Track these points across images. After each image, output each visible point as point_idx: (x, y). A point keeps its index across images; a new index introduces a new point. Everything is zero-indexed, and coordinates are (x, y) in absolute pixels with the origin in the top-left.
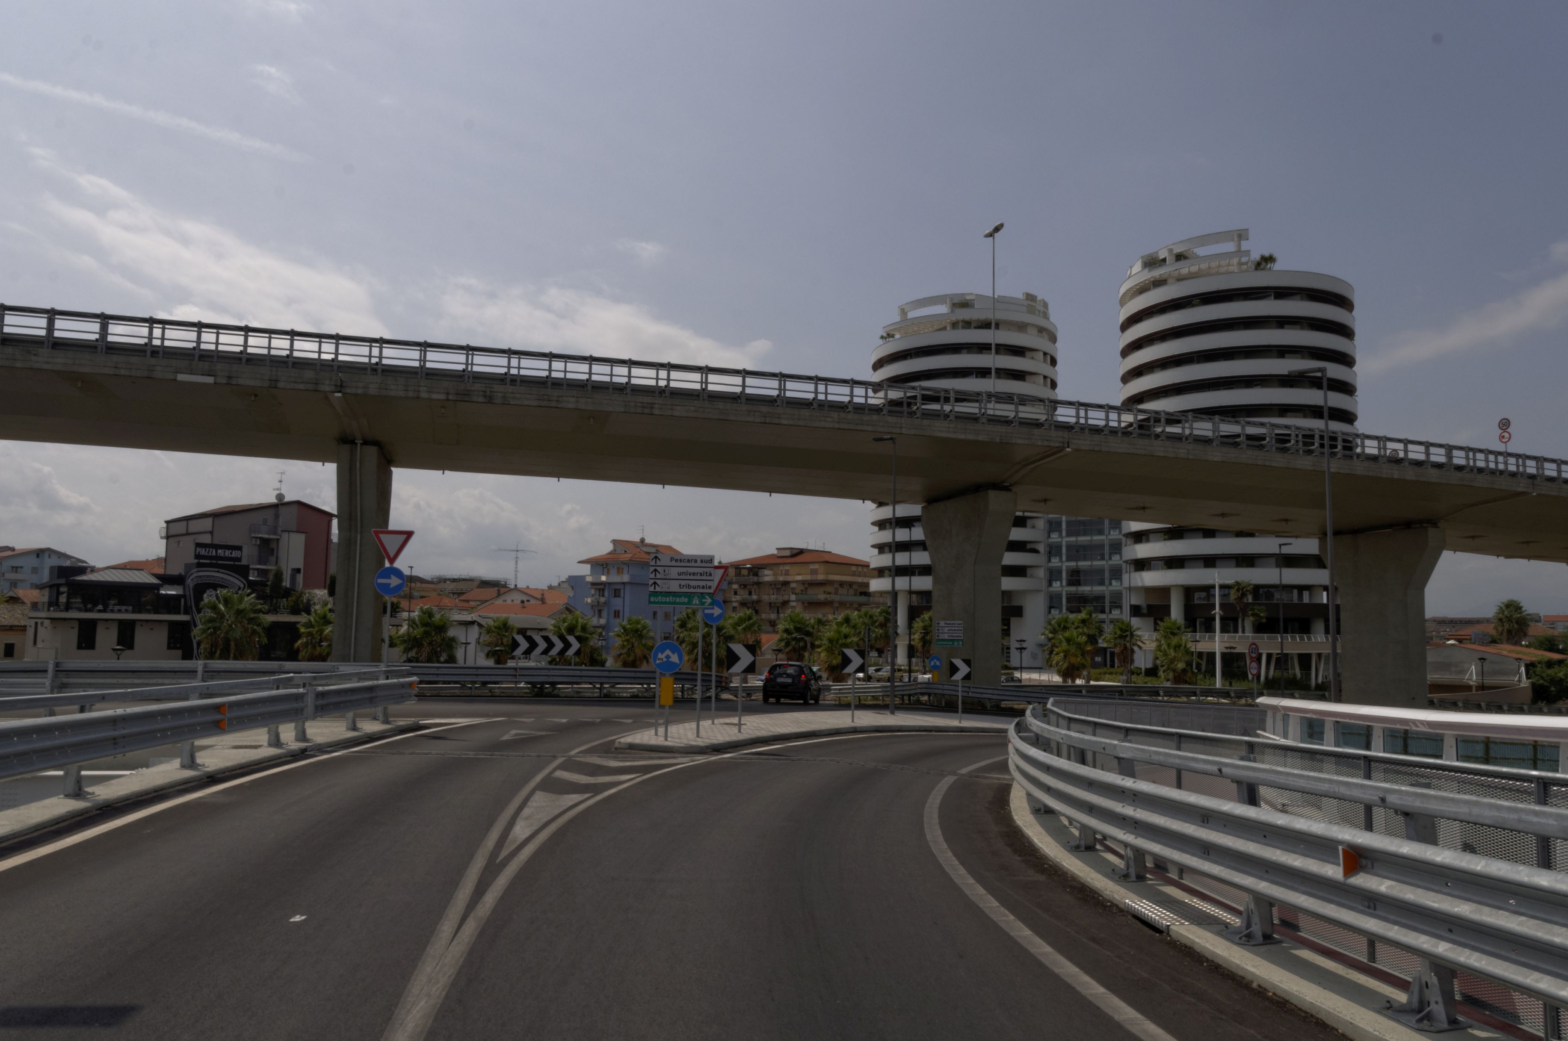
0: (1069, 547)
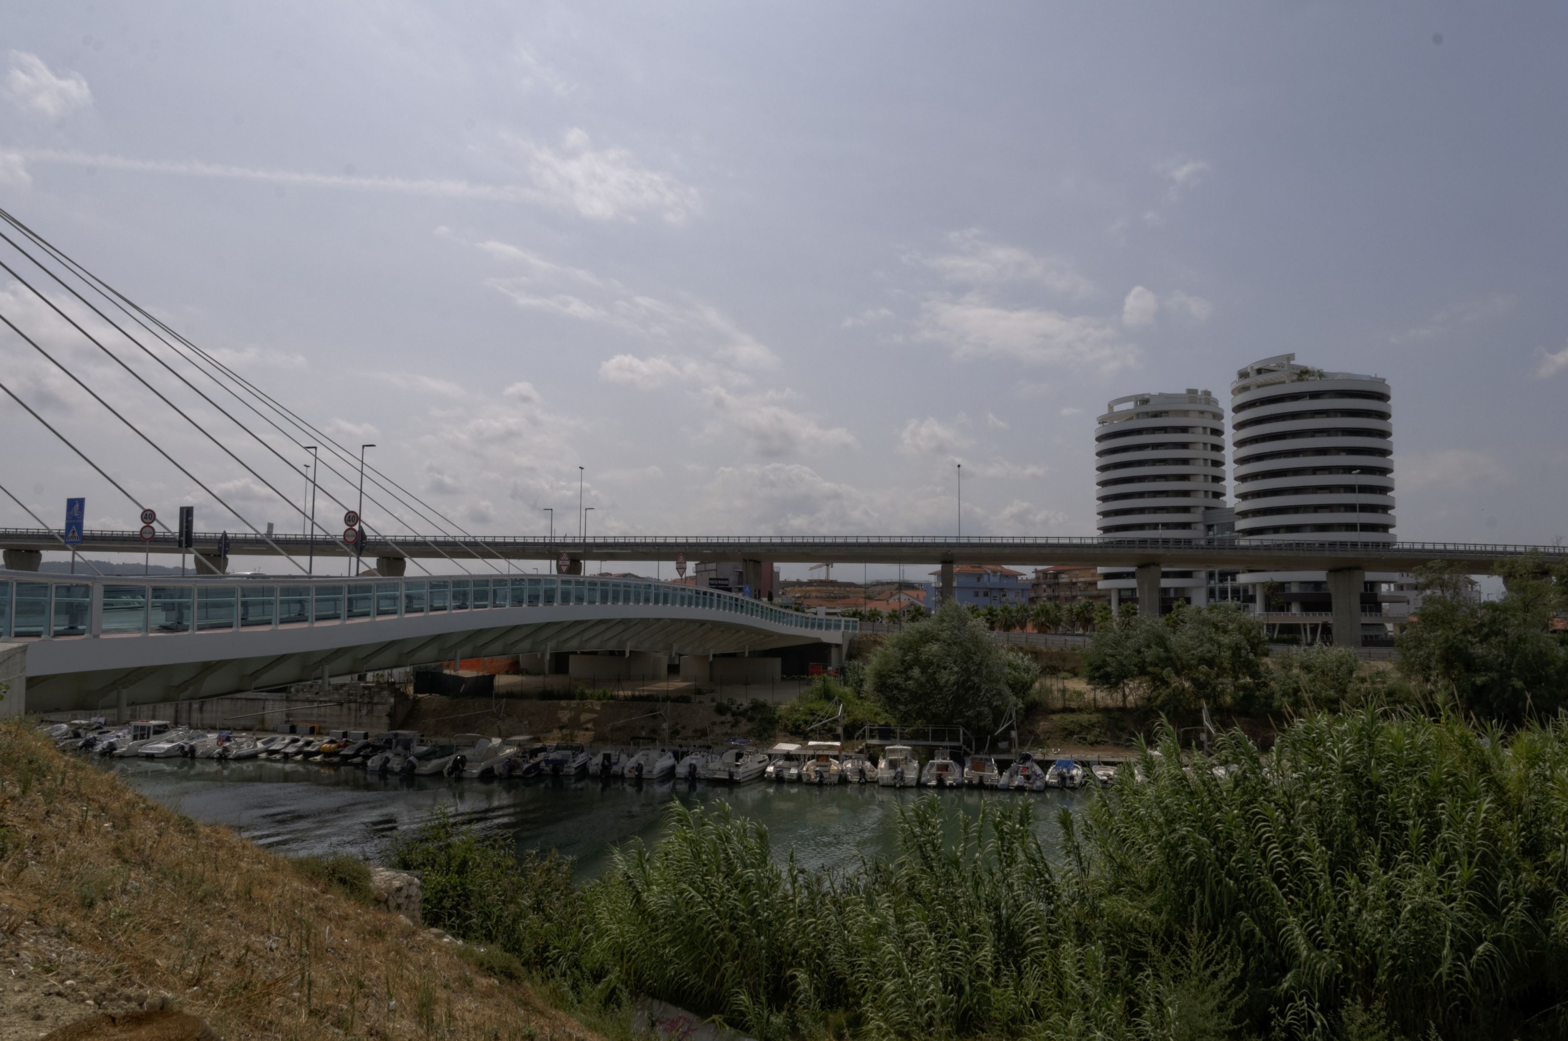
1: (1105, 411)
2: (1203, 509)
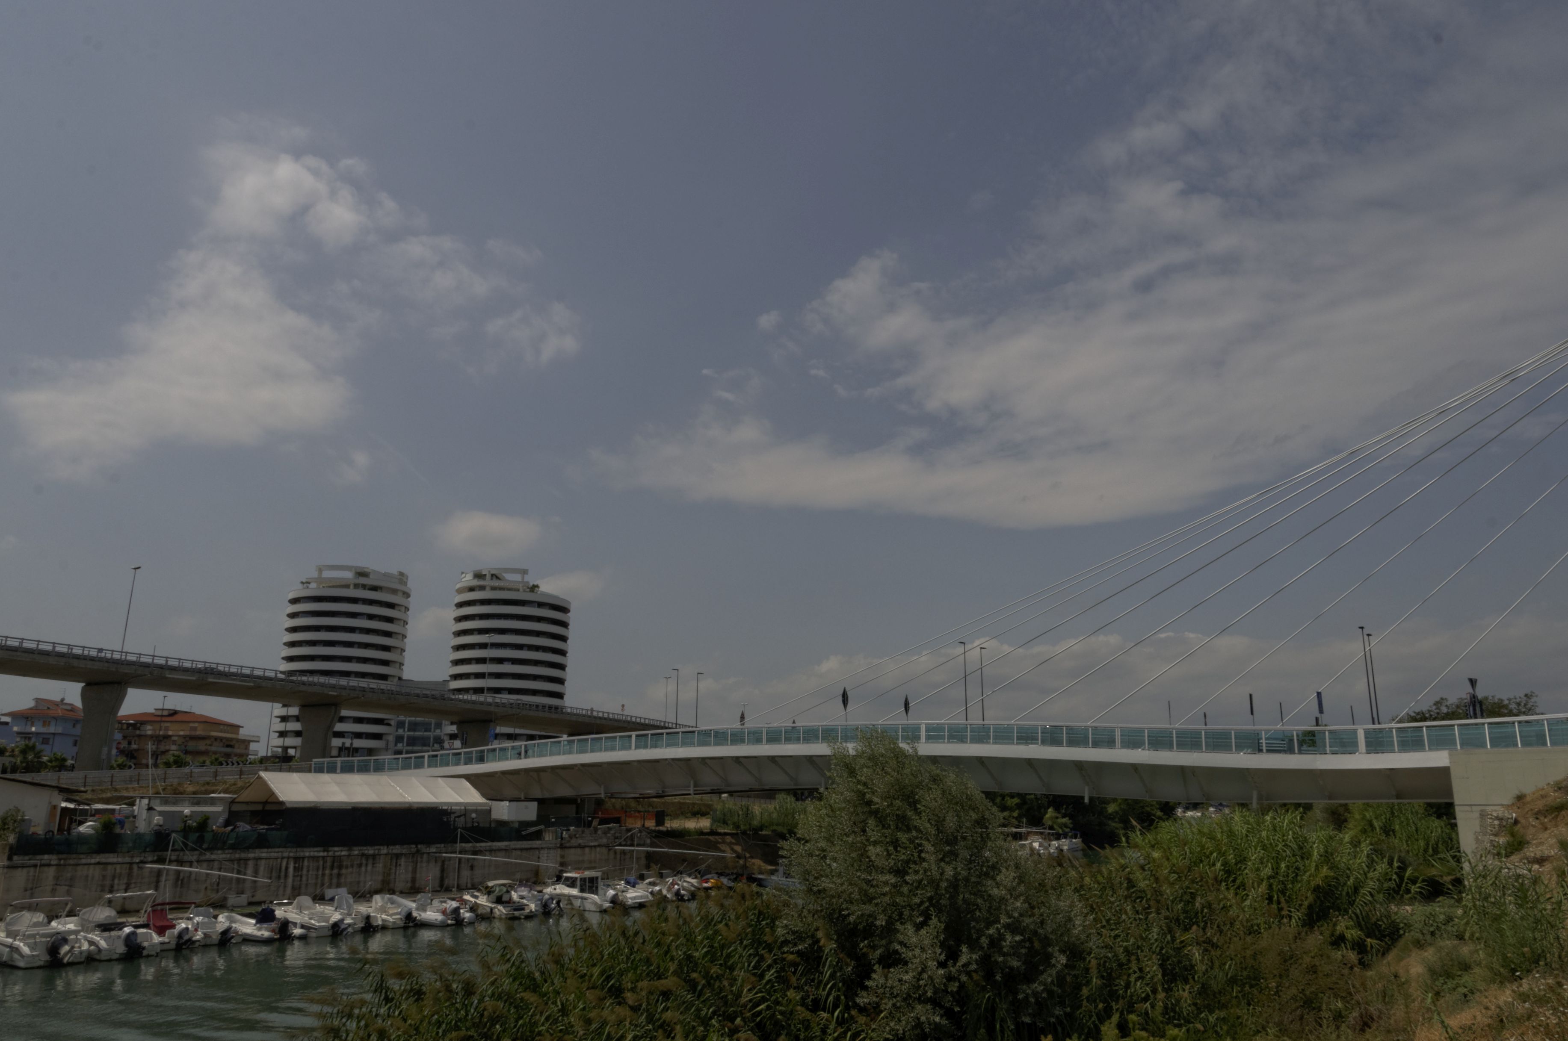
0: (410, 723)
2: (397, 679)
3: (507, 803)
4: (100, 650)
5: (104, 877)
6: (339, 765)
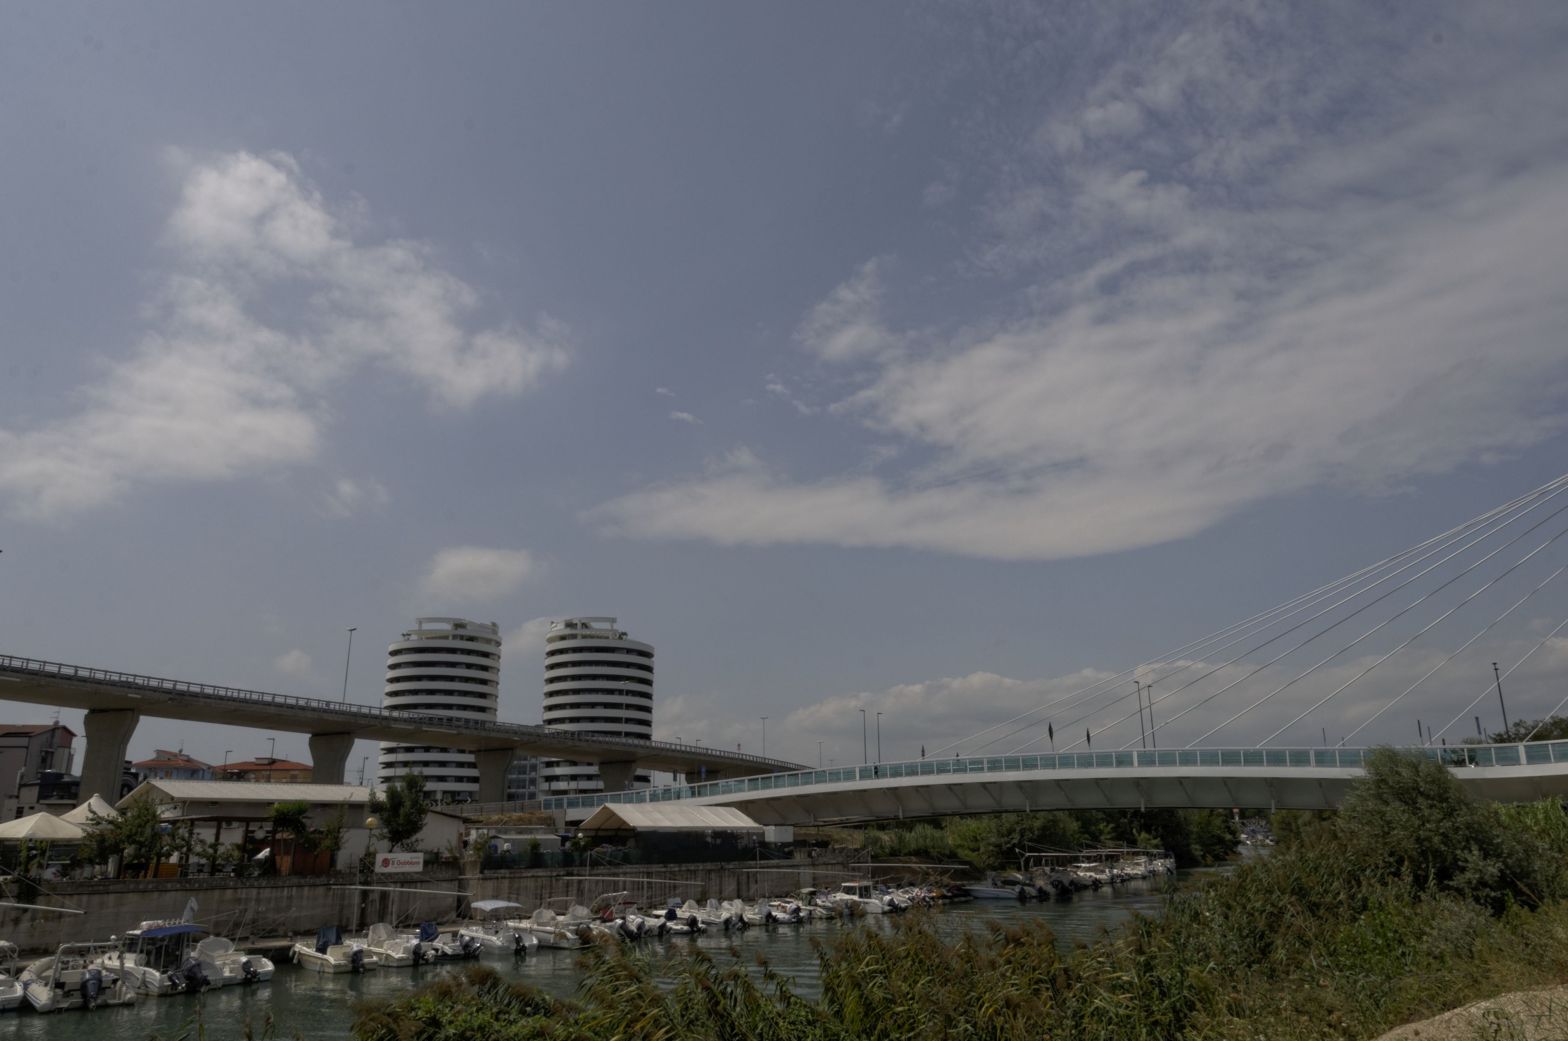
1: (416, 627)
3: (773, 828)
4: (328, 703)
5: (536, 887)
6: (565, 801)
